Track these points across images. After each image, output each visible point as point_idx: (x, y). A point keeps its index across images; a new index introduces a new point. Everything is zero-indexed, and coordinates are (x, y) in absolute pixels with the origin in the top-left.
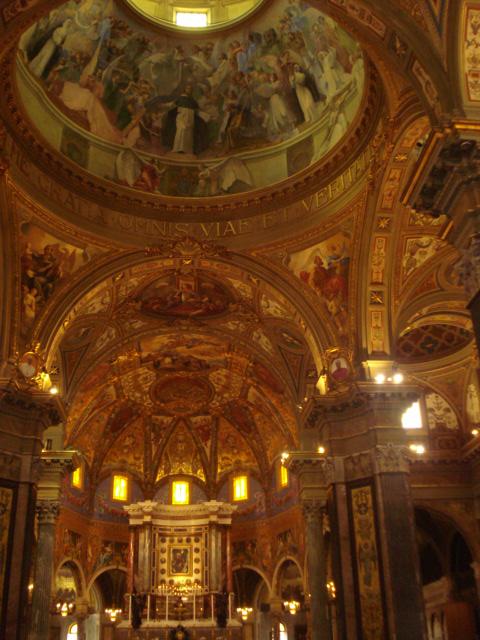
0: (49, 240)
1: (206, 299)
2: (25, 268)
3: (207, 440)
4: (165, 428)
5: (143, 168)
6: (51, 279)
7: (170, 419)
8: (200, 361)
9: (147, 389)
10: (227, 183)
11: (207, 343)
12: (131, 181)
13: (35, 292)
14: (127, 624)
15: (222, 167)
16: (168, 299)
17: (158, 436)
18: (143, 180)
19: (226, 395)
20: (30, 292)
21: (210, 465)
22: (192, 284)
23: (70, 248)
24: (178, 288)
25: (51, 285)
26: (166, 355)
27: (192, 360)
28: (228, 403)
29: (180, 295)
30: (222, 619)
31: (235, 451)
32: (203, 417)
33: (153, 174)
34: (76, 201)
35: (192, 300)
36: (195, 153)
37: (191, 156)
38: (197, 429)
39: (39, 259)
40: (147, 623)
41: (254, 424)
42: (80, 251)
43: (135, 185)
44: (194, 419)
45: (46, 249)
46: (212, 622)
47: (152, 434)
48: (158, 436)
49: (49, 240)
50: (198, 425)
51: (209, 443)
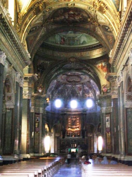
0: (42, 61)
2: (38, 68)
3: (80, 91)
5: (62, 38)
6: (43, 69)
10: (81, 43)
12: (59, 43)
13: (40, 72)
14: (62, 137)
15: (81, 37)
18: (62, 42)
20: (39, 73)
23: (47, 62)
25: (43, 70)
28: (86, 82)
30: (84, 137)
32: (80, 85)
33: (64, 40)
34: (47, 51)
36: (74, 33)
37: (73, 33)
38: (78, 88)
39: (40, 66)
40: (66, 137)
41: (93, 87)
42: (49, 62)
43: (60, 44)
45: (42, 63)
46: (81, 137)
49: (42, 61)
50: (78, 87)
51: (81, 91)
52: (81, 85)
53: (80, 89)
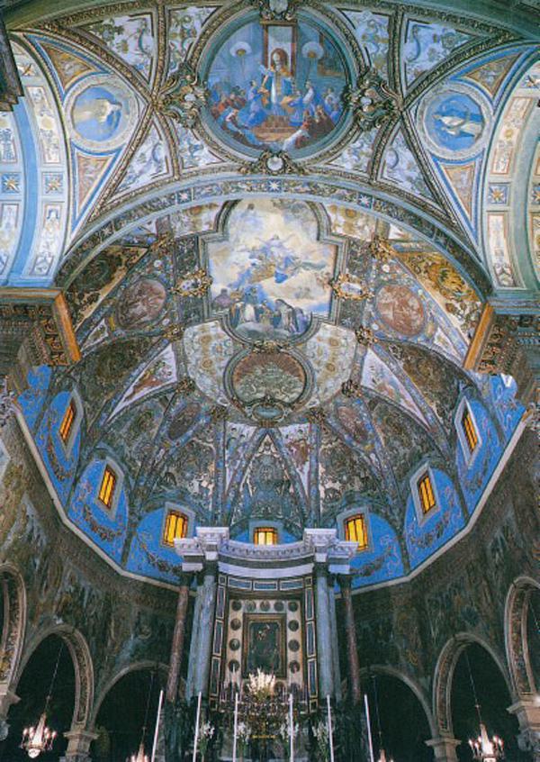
1: (310, 94)
3: (304, 463)
4: (245, 444)
7: (252, 429)
8: (293, 313)
9: (220, 373)
11: (307, 265)
16: (251, 96)
17: (234, 458)
19: (329, 384)
21: (308, 502)
22: (287, 47)
24: (266, 66)
26: (248, 297)
27: (284, 310)
29: (268, 87)
31: (345, 478)
35: (287, 99)
44: (285, 430)
47: (226, 452)
48: (234, 458)
51: (306, 467)
52: (305, 426)
53: (304, 453)
